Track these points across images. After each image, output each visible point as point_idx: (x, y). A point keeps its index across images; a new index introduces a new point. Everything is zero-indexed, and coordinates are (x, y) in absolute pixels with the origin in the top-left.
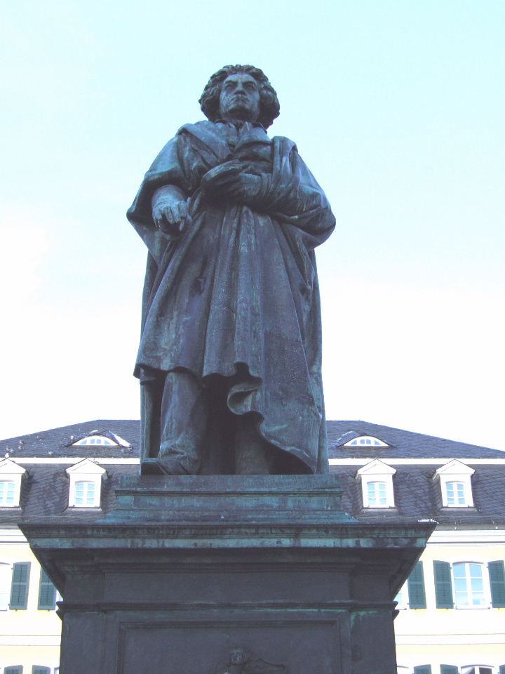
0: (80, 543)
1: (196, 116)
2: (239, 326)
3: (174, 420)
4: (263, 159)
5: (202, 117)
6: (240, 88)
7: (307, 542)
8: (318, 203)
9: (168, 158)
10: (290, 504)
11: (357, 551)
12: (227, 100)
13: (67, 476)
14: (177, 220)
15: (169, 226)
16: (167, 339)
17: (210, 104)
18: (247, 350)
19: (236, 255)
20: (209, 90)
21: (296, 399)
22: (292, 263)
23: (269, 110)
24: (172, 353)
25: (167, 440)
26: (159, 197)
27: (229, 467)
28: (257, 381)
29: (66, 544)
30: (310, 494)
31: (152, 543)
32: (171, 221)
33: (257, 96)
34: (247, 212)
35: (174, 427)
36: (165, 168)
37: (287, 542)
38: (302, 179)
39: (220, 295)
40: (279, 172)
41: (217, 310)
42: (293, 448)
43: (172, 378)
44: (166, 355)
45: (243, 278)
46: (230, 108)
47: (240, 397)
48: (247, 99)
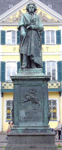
0: (16, 78)
12: (30, 10)
16: (23, 50)
18: (33, 53)
19: (31, 39)
22: (38, 37)
23: (35, 10)
27: (31, 67)
28: (34, 56)
31: (23, 78)
33: (34, 9)
36: (22, 23)
39: (29, 45)
41: (29, 47)
43: (24, 55)
47: (32, 58)
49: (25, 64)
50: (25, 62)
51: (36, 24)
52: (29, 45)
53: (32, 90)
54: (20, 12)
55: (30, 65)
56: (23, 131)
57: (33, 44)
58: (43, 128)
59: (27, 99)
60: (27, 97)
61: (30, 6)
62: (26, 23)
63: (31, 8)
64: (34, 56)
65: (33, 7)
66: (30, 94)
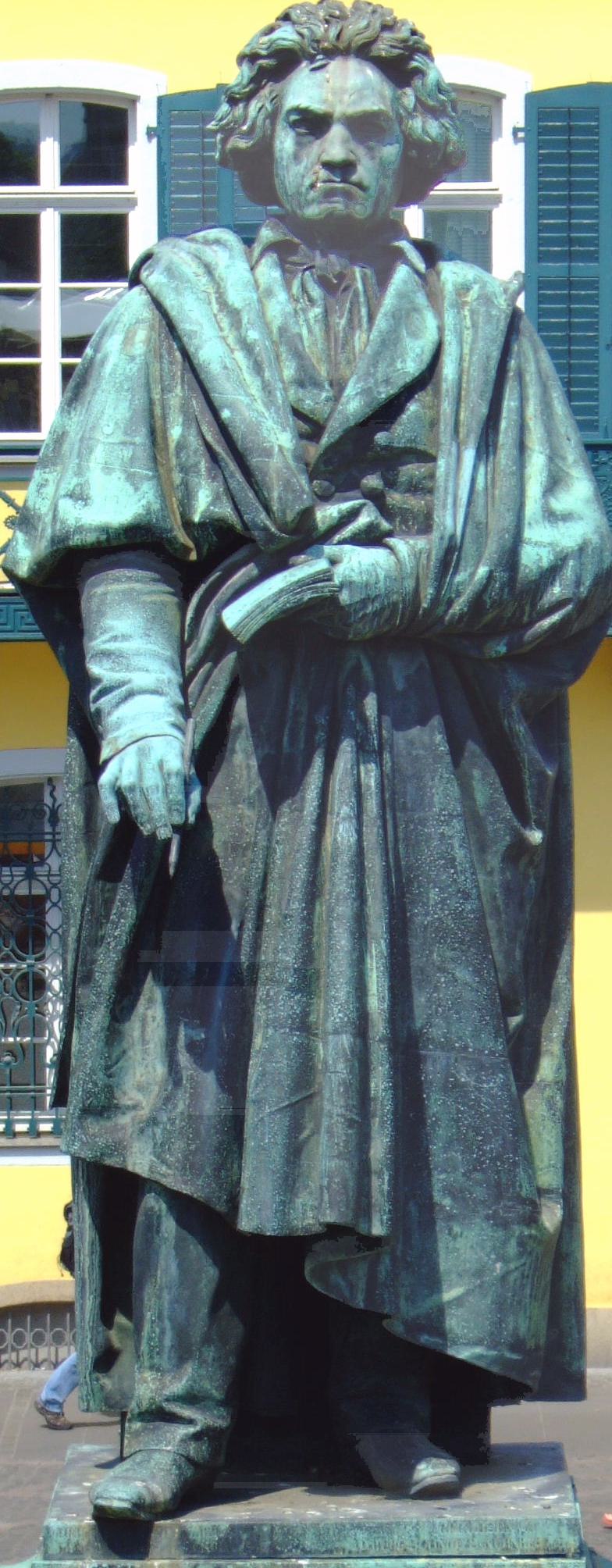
3: (167, 1324)
6: (335, 145)
8: (568, 593)
14: (163, 833)
20: (239, 110)
21: (488, 1218)
24: (158, 1131)
25: (152, 1368)
26: (101, 614)
32: (146, 830)
33: (391, 152)
34: (358, 668)
35: (168, 1341)
40: (452, 537)
42: (478, 1350)
43: (151, 1201)
44: (142, 1131)
46: (313, 211)
48: (359, 185)
50: (183, 1353)
51: (449, 520)
55: (390, 461)
62: (204, 501)
65: (365, 127)
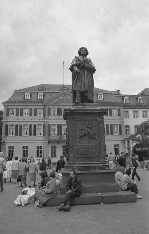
1: (77, 55)
2: (86, 85)
4: (87, 62)
5: (78, 55)
6: (84, 51)
7: (95, 111)
9: (75, 61)
10: (92, 107)
11: (99, 112)
12: (82, 52)
13: (38, 94)
15: (76, 73)
17: (79, 53)
18: (87, 88)
23: (87, 54)
28: (88, 92)
29: (69, 112)
30: (94, 106)
31: (79, 111)
36: (75, 63)
37: (93, 111)
38: (92, 65)
39: (83, 81)
45: (86, 78)
49: (78, 99)
50: (78, 98)
52: (83, 81)
53: (88, 125)
54: (59, 98)
56: (79, 169)
57: (86, 81)
58: (101, 165)
59: (82, 133)
60: (83, 131)
61: (82, 49)
62: (79, 63)
63: (84, 51)
64: (88, 92)
65: (85, 51)
66: (86, 129)
